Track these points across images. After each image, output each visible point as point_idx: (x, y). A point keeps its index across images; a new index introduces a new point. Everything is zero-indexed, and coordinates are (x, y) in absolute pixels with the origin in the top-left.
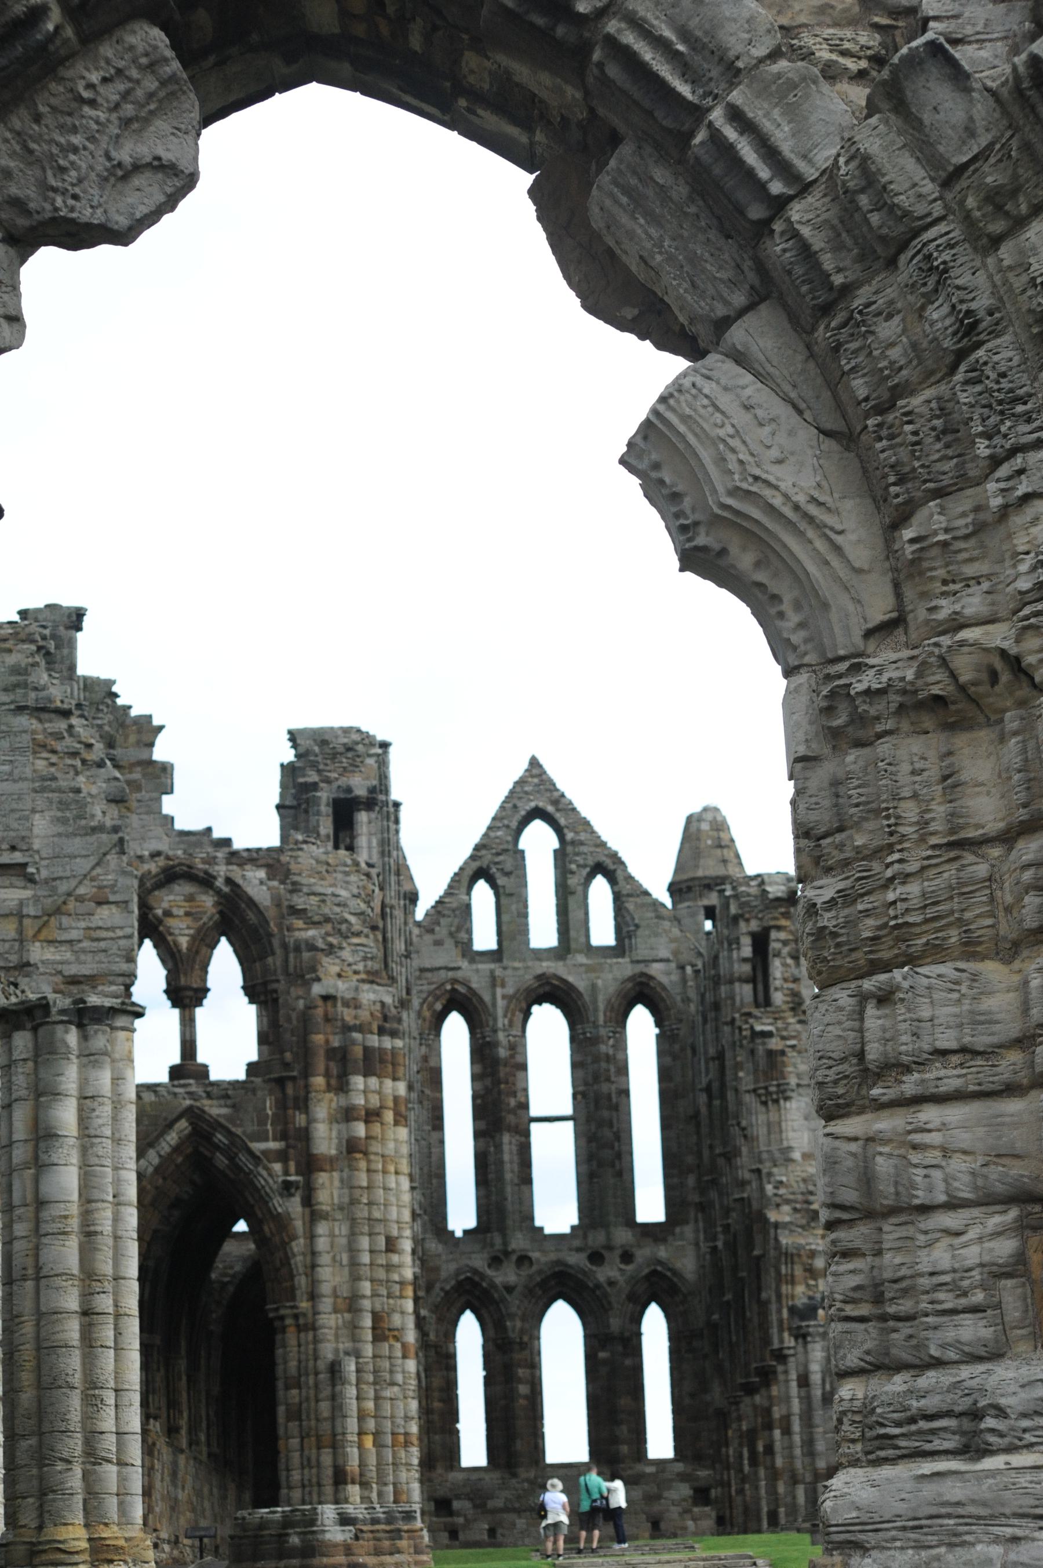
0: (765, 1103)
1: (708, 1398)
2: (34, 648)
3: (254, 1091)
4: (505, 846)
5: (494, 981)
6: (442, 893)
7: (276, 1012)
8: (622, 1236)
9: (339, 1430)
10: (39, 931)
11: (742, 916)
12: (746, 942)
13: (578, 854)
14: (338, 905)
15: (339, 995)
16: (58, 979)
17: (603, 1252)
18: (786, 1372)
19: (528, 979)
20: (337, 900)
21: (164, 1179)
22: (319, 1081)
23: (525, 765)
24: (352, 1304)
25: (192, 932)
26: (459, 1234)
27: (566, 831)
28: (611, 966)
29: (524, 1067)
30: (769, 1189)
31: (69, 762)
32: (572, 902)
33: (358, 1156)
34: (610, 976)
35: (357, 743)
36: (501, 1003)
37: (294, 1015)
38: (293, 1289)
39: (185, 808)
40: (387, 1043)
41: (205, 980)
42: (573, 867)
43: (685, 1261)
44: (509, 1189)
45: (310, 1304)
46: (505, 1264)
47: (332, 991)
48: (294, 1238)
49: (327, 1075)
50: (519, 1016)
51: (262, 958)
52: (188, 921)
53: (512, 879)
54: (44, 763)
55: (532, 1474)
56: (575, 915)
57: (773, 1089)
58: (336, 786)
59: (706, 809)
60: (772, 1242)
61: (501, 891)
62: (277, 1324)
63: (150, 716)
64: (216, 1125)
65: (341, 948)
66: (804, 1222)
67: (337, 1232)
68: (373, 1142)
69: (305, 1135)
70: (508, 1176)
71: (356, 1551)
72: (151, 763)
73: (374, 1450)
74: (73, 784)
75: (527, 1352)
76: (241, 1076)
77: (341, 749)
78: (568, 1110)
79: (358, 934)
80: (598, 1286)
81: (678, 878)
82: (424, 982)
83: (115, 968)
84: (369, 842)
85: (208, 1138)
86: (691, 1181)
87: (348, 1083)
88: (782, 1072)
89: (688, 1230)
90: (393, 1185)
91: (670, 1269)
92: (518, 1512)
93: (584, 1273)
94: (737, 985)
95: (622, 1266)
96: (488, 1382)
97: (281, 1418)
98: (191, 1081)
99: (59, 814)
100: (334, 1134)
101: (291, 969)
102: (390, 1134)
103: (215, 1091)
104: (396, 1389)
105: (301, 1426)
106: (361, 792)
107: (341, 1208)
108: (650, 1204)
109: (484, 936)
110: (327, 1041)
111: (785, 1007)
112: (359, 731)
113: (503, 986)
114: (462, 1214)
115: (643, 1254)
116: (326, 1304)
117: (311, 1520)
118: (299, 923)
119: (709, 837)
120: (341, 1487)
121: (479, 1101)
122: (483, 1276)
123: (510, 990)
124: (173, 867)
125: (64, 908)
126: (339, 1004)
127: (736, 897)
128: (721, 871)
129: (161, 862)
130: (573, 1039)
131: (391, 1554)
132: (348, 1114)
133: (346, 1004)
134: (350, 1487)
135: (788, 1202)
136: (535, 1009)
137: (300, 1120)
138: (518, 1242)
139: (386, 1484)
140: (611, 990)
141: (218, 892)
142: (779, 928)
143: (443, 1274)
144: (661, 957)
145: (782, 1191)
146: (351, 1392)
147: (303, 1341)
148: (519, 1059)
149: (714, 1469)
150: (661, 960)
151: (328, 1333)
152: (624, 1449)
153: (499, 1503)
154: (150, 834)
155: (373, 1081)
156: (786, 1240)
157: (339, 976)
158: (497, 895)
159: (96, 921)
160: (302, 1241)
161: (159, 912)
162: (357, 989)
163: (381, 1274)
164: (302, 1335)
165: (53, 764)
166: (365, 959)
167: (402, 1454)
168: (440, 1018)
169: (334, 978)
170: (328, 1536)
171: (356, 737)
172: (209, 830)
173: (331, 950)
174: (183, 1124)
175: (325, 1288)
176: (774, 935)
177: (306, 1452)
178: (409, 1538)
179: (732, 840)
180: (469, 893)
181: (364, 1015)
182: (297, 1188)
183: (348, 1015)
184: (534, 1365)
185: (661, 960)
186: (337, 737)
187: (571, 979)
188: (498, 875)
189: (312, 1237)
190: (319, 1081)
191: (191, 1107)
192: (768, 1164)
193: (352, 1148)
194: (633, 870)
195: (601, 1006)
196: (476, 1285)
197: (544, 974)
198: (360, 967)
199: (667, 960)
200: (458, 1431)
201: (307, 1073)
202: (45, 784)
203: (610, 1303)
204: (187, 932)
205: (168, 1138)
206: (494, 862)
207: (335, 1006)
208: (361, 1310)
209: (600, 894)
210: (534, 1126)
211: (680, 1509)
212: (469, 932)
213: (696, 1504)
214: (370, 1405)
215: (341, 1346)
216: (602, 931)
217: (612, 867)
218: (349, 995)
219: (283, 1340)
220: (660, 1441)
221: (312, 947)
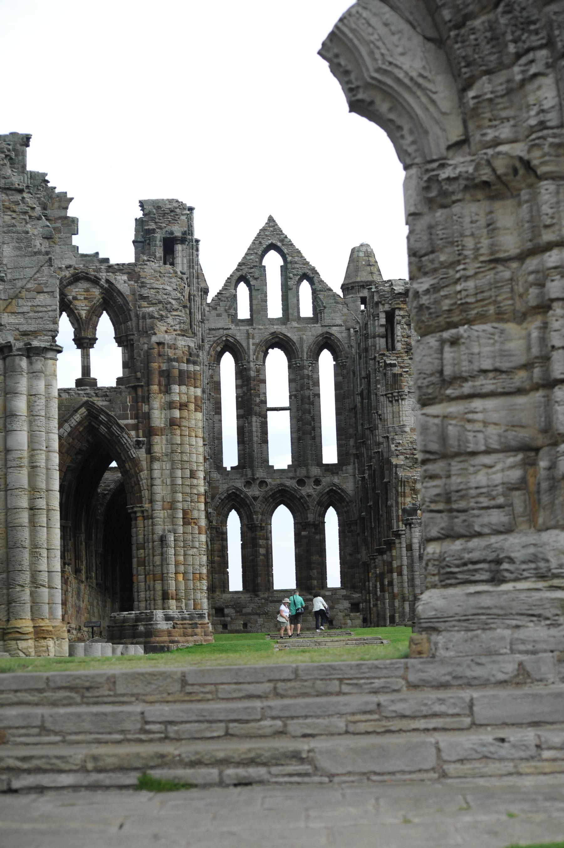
0: (391, 402)
1: (359, 556)
2: (4, 156)
3: (121, 393)
4: (255, 264)
5: (248, 336)
6: (221, 288)
7: (132, 351)
8: (315, 471)
9: (165, 571)
10: (7, 307)
11: (380, 302)
12: (383, 316)
13: (294, 269)
14: (166, 294)
15: (166, 342)
16: (17, 333)
17: (306, 480)
18: (400, 543)
19: (266, 335)
20: (165, 292)
21: (73, 439)
22: (155, 388)
23: (266, 221)
24: (172, 506)
25: (88, 308)
26: (229, 469)
27: (287, 256)
28: (310, 328)
29: (264, 381)
30: (393, 446)
31: (22, 217)
32: (290, 294)
33: (176, 427)
34: (310, 334)
35: (176, 208)
36: (252, 347)
37: (142, 353)
38: (141, 497)
39: (85, 242)
40: (191, 368)
41: (95, 334)
42: (291, 275)
43: (348, 484)
44: (255, 446)
45: (150, 505)
46: (253, 485)
47: (162, 340)
48: (142, 470)
49: (159, 384)
50: (262, 354)
51: (125, 322)
52: (86, 302)
54: (9, 217)
55: (266, 595)
56: (292, 301)
57: (395, 394)
58: (165, 231)
59: (362, 245)
60: (394, 474)
61: (253, 287)
62: (132, 515)
63: (66, 193)
64: (101, 410)
65: (167, 317)
66: (411, 464)
67: (164, 468)
68: (183, 420)
69: (148, 416)
70: (255, 439)
71: (173, 634)
72: (67, 218)
73: (183, 582)
74: (24, 229)
75: (264, 531)
76: (114, 385)
77: (168, 211)
78: (287, 404)
79: (176, 310)
80: (302, 497)
81: (347, 282)
83: (47, 327)
84: (182, 260)
85: (96, 418)
86: (352, 442)
87: (170, 389)
88: (400, 385)
89: (350, 468)
90: (194, 443)
91: (340, 489)
92: (259, 615)
94: (377, 338)
96: (243, 547)
97: (135, 565)
98: (87, 387)
99: (17, 245)
100: (163, 416)
101: (141, 329)
102: (193, 416)
103: (100, 392)
104: (195, 550)
105: (145, 569)
106: (178, 234)
107: (167, 455)
108: (330, 454)
109: (243, 311)
110: (160, 367)
111: (402, 351)
112: (177, 201)
113: (253, 338)
114: (230, 458)
115: (326, 480)
116: (158, 505)
117: (150, 618)
118: (145, 304)
119: (364, 260)
120: (166, 601)
121: (240, 399)
122: (241, 492)
123: (257, 341)
124: (78, 273)
125: (20, 295)
126: (166, 347)
127: (377, 292)
128: (370, 278)
129: (72, 271)
130: (290, 367)
131: (192, 636)
132: (170, 405)
133: (170, 347)
134: (170, 601)
135: (402, 454)
136: (270, 351)
137: (145, 408)
138: (260, 474)
139: (189, 600)
140: (311, 341)
141: (102, 287)
142: (400, 309)
144: (338, 323)
145: (399, 448)
146: (172, 551)
147: (146, 525)
148: (261, 377)
150: (337, 326)
151: (159, 521)
152: (315, 582)
153: (249, 610)
154: (66, 256)
155: (184, 388)
156: (401, 473)
157: (166, 332)
158: (250, 290)
159: (37, 302)
160: (146, 472)
161: (71, 297)
162: (175, 339)
163: (188, 490)
164: (146, 521)
165: (14, 218)
166: (180, 323)
167: (198, 584)
168: (220, 355)
169: (163, 333)
170: (159, 626)
171: (176, 205)
172: (97, 254)
173: (162, 318)
174: (83, 410)
175: (158, 497)
176: (397, 312)
177: (148, 583)
178: (202, 628)
179: (376, 262)
180: (235, 289)
181: (179, 353)
182: (143, 444)
183: (171, 353)
184: (268, 538)
186: (165, 205)
187: (289, 335)
188: (251, 279)
189: (151, 470)
190: (155, 388)
191: (87, 402)
192: (392, 434)
193: (172, 423)
194: (323, 277)
195: (305, 350)
198: (177, 327)
199: (341, 326)
201: (148, 384)
202: (10, 229)
203: (308, 506)
204: (85, 308)
205: (75, 418)
207: (164, 348)
208: (176, 509)
209: (305, 289)
210: (269, 413)
211: (343, 614)
212: (236, 309)
213: (352, 612)
214: (181, 558)
215: (166, 527)
216: (306, 309)
217: (312, 275)
218: (171, 342)
219: (136, 524)
220: (334, 579)
221: (152, 317)
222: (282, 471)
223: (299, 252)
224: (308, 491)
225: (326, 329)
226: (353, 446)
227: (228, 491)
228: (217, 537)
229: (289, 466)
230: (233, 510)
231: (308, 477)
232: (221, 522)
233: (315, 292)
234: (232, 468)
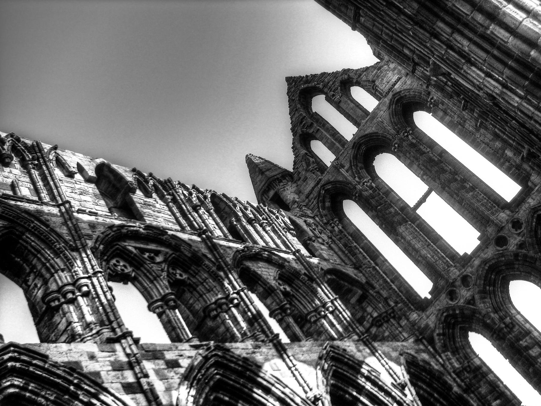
19: (351, 152)
26: (429, 297)
46: (458, 291)
50: (364, 172)
53: (315, 125)
75: (517, 327)
82: (313, 200)
89: (534, 178)
93: (502, 255)
95: (519, 231)
108: (507, 188)
113: (343, 166)
123: (347, 166)
143: (432, 325)
150: (396, 82)
185: (396, 82)
196: (454, 316)
199: (399, 79)
203: (532, 258)
206: (306, 129)
217: (346, 77)
222: (478, 249)
223: (325, 73)
224: (516, 242)
225: (391, 94)
227: (440, 320)
229: (479, 239)
231: (501, 229)
233: (358, 84)
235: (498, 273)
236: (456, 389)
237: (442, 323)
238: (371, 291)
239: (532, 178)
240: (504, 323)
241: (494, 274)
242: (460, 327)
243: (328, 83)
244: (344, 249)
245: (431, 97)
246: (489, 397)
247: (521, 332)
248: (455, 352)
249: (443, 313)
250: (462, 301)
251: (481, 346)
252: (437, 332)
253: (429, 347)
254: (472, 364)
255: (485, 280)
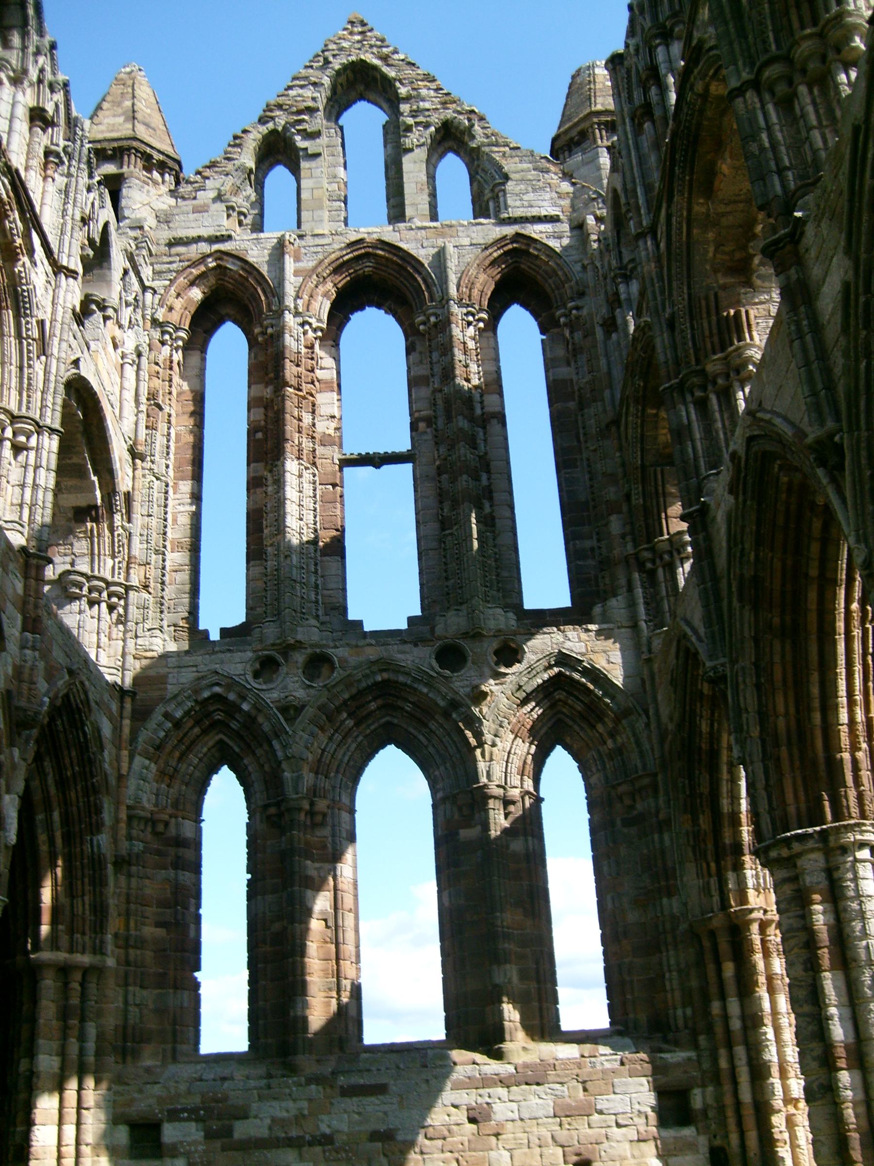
17: (465, 644)
26: (215, 636)
27: (398, 84)
34: (466, 241)
46: (284, 670)
75: (326, 832)
78: (404, 444)
86: (616, 525)
113: (297, 259)
121: (259, 435)
123: (308, 264)
149: (696, 1047)
196: (232, 709)
197: (361, 241)
200: (197, 985)
226: (623, 536)
227: (197, 692)
228: (159, 853)
229: (411, 620)
230: (225, 770)
232: (176, 805)
234: (224, 632)
235: (388, 708)
236: (103, 839)
237: (196, 701)
238: (117, 517)
239: (613, 602)
240: (312, 804)
241: (380, 702)
242: (221, 741)
243: (423, 100)
244: (143, 399)
245: (579, 303)
246: (150, 911)
247: (325, 847)
248: (167, 775)
249: (218, 684)
250: (275, 695)
251: (225, 809)
252: (171, 708)
253: (127, 722)
254: (177, 825)
255: (353, 698)
